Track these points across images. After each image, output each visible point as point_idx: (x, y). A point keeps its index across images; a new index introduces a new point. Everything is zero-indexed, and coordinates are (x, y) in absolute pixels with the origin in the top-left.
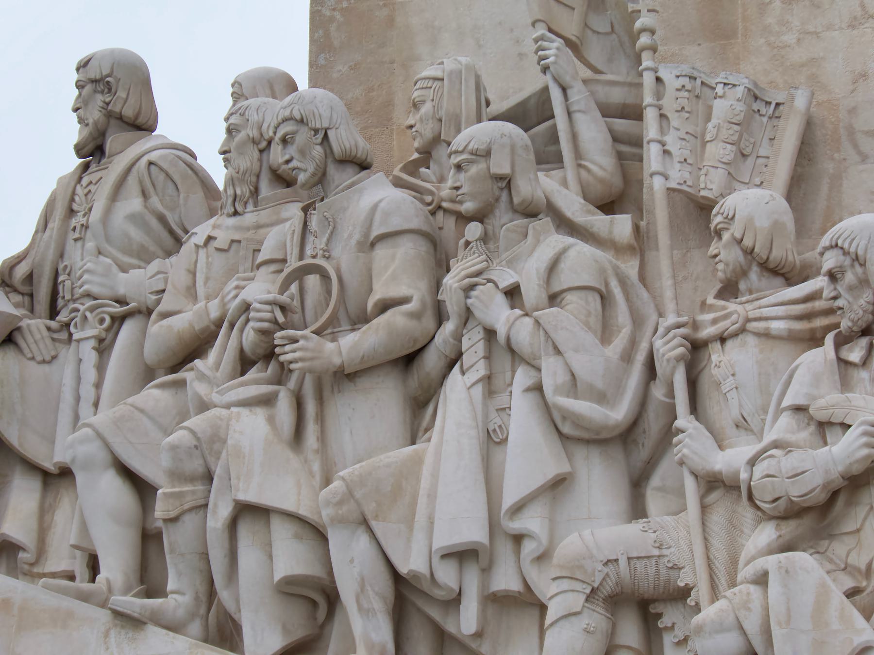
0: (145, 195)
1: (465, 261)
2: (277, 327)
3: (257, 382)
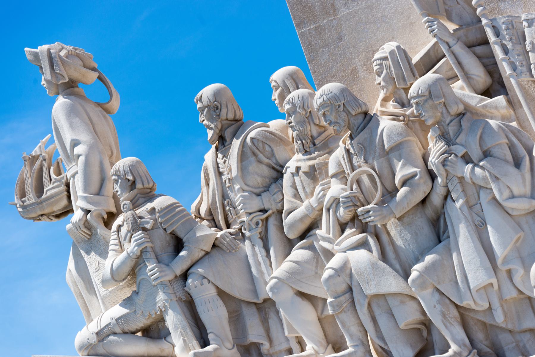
0: (254, 154)
1: (435, 148)
2: (356, 207)
3: (353, 234)
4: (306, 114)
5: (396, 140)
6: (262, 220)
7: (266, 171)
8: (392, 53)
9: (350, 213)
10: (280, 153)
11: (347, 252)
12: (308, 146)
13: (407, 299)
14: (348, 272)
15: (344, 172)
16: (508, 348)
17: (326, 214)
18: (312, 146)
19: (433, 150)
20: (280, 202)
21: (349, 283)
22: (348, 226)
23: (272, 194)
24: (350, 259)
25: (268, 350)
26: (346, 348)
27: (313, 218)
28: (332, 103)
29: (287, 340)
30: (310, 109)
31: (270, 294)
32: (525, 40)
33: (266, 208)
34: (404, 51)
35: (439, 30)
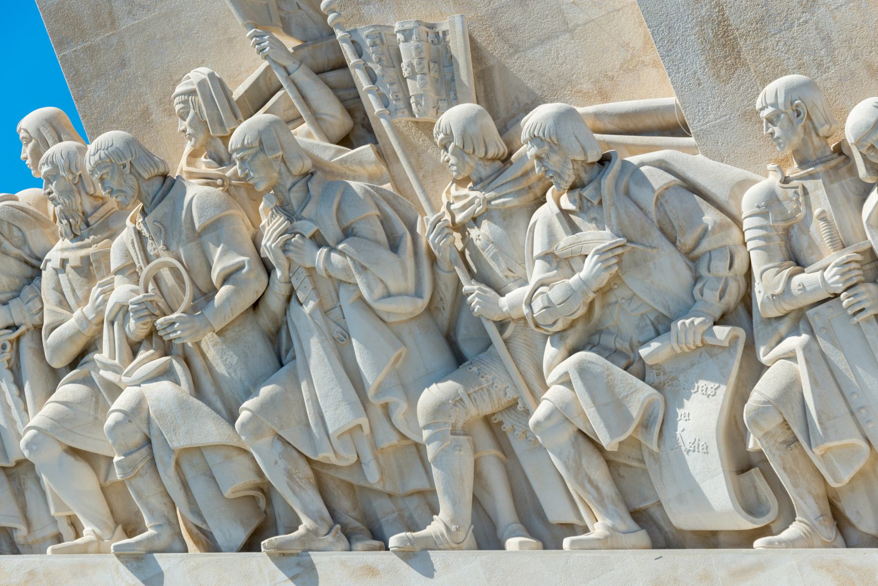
1: (271, 225)
2: (153, 317)
3: (150, 359)
4: (74, 178)
5: (212, 215)
6: (11, 342)
7: (15, 267)
8: (202, 83)
9: (145, 327)
10: (36, 239)
11: (142, 385)
12: (77, 227)
13: (234, 453)
14: (144, 415)
15: (134, 265)
16: (387, 520)
17: (109, 330)
18: (85, 227)
19: (267, 228)
20: (37, 314)
21: (146, 432)
22: (142, 347)
23: (26, 302)
24: (146, 395)
25: (25, 537)
26: (145, 530)
27: (88, 335)
28: (113, 161)
29: (54, 521)
30: (80, 172)
31: (26, 454)
32: (400, 61)
33: (17, 323)
34: (220, 80)
35: (271, 48)
